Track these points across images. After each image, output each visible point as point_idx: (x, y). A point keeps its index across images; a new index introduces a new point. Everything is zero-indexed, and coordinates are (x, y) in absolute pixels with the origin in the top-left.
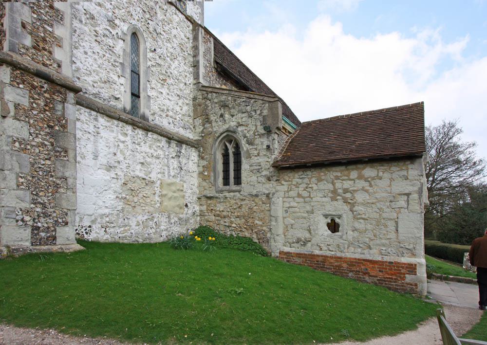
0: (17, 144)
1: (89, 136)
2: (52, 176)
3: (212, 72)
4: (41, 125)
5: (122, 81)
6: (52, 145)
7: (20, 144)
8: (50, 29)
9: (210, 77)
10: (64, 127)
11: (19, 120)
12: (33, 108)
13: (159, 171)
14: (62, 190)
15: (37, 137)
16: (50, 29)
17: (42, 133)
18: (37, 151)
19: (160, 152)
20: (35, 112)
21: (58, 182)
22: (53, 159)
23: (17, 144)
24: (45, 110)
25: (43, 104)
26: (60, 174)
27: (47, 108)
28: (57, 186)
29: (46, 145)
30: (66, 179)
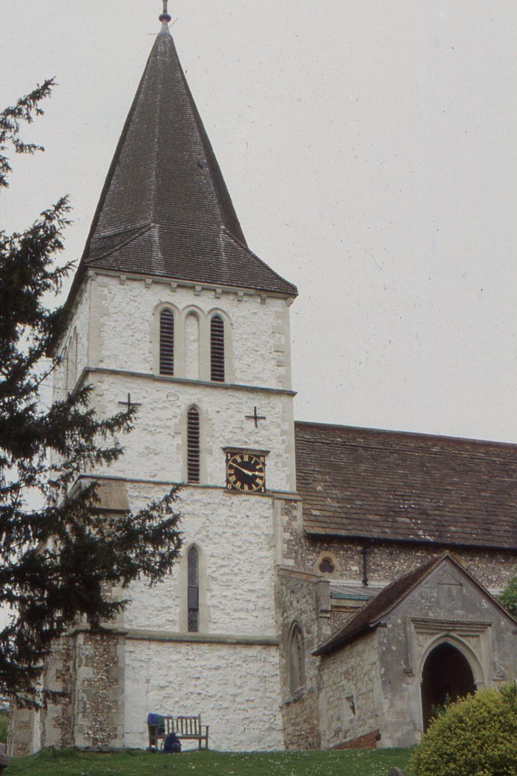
0: (86, 682)
1: (142, 664)
2: (107, 701)
3: (301, 543)
4: (101, 665)
5: (178, 601)
6: (108, 678)
7: (88, 681)
8: (109, 594)
9: (296, 552)
10: (116, 663)
11: (87, 666)
12: (96, 656)
13: (219, 683)
14: (113, 711)
15: (98, 674)
16: (109, 594)
17: (101, 671)
18: (98, 684)
19: (222, 663)
20: (97, 658)
21: (111, 704)
22: (107, 688)
23: (86, 682)
24: (104, 654)
25: (102, 651)
26: (112, 699)
27: (105, 653)
28: (110, 708)
29: (103, 679)
30: (117, 702)
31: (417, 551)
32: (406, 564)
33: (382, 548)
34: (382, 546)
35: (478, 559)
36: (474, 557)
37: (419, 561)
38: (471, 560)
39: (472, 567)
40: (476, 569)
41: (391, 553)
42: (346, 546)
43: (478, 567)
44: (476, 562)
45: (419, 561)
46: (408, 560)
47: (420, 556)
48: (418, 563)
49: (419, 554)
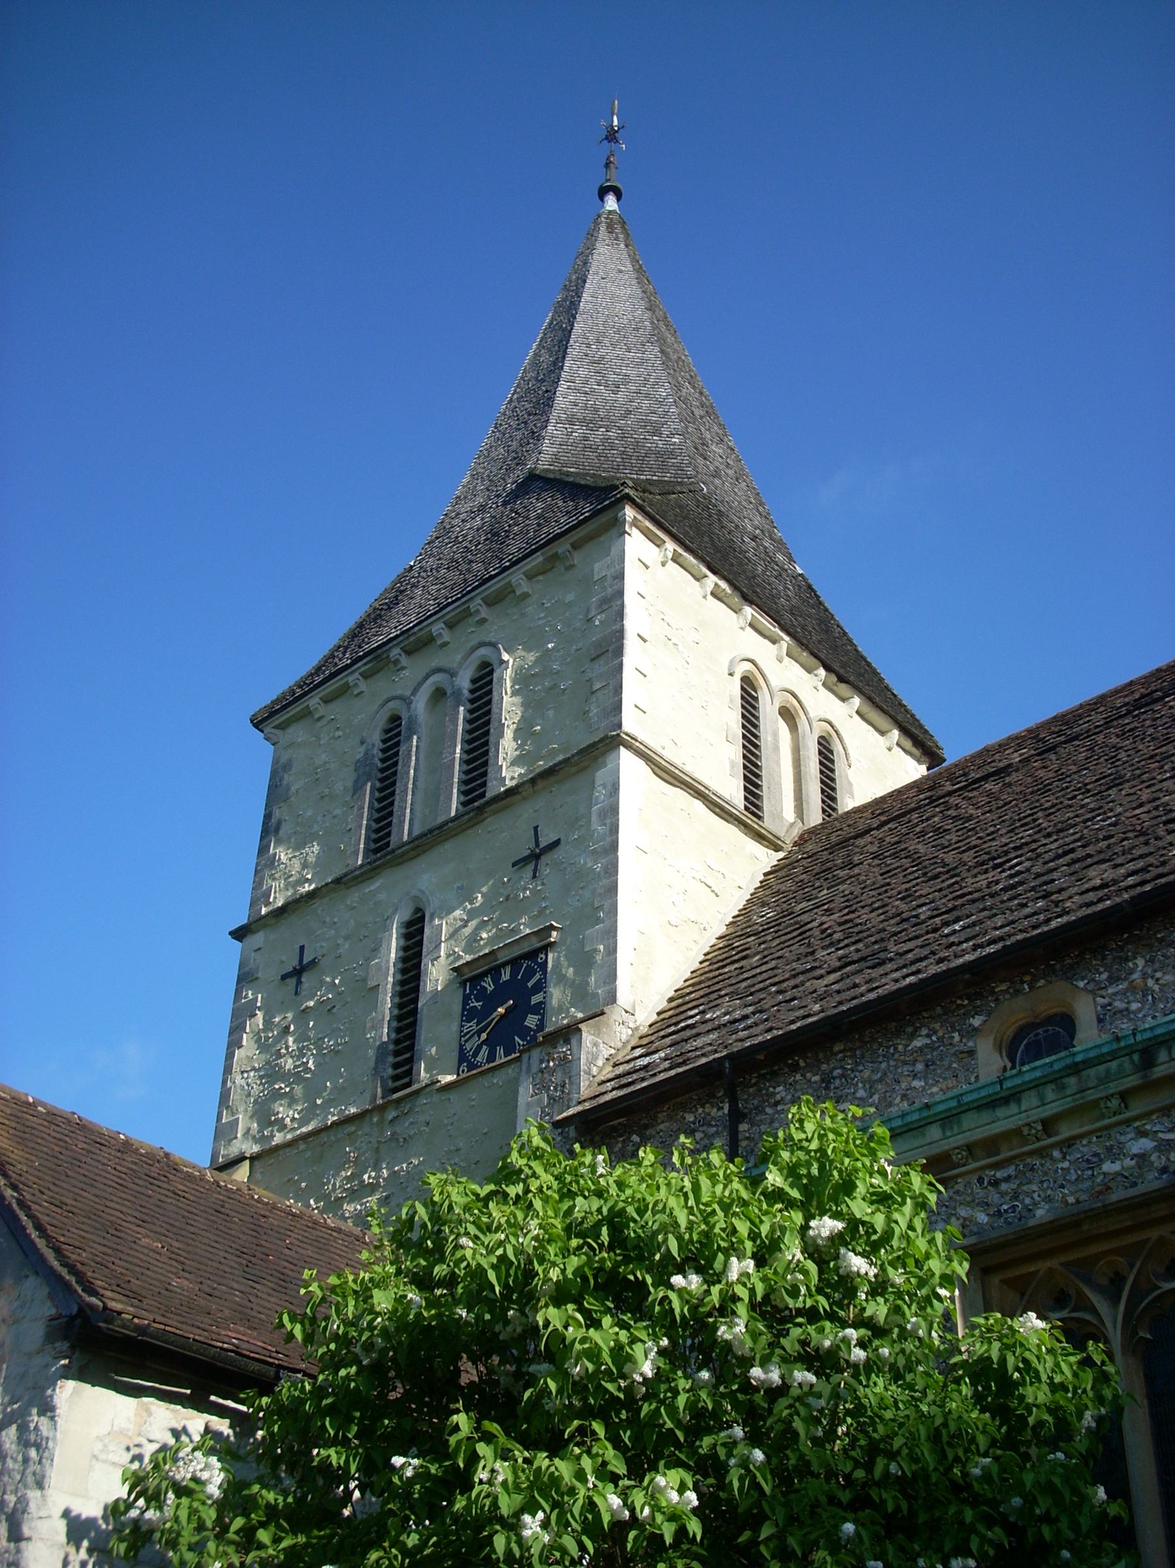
31: (913, 1036)
32: (876, 1097)
33: (798, 1077)
34: (795, 1068)
35: (1140, 962)
36: (1127, 960)
37: (920, 1067)
38: (1113, 980)
39: (1118, 1004)
40: (1134, 1006)
41: (827, 1080)
42: (690, 1118)
43: (1146, 991)
44: (1135, 976)
45: (920, 1067)
46: (880, 1080)
47: (921, 1049)
48: (915, 1077)
49: (918, 1043)
